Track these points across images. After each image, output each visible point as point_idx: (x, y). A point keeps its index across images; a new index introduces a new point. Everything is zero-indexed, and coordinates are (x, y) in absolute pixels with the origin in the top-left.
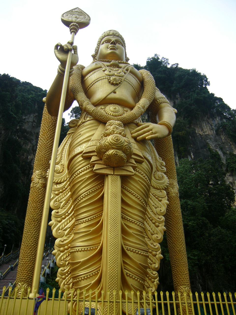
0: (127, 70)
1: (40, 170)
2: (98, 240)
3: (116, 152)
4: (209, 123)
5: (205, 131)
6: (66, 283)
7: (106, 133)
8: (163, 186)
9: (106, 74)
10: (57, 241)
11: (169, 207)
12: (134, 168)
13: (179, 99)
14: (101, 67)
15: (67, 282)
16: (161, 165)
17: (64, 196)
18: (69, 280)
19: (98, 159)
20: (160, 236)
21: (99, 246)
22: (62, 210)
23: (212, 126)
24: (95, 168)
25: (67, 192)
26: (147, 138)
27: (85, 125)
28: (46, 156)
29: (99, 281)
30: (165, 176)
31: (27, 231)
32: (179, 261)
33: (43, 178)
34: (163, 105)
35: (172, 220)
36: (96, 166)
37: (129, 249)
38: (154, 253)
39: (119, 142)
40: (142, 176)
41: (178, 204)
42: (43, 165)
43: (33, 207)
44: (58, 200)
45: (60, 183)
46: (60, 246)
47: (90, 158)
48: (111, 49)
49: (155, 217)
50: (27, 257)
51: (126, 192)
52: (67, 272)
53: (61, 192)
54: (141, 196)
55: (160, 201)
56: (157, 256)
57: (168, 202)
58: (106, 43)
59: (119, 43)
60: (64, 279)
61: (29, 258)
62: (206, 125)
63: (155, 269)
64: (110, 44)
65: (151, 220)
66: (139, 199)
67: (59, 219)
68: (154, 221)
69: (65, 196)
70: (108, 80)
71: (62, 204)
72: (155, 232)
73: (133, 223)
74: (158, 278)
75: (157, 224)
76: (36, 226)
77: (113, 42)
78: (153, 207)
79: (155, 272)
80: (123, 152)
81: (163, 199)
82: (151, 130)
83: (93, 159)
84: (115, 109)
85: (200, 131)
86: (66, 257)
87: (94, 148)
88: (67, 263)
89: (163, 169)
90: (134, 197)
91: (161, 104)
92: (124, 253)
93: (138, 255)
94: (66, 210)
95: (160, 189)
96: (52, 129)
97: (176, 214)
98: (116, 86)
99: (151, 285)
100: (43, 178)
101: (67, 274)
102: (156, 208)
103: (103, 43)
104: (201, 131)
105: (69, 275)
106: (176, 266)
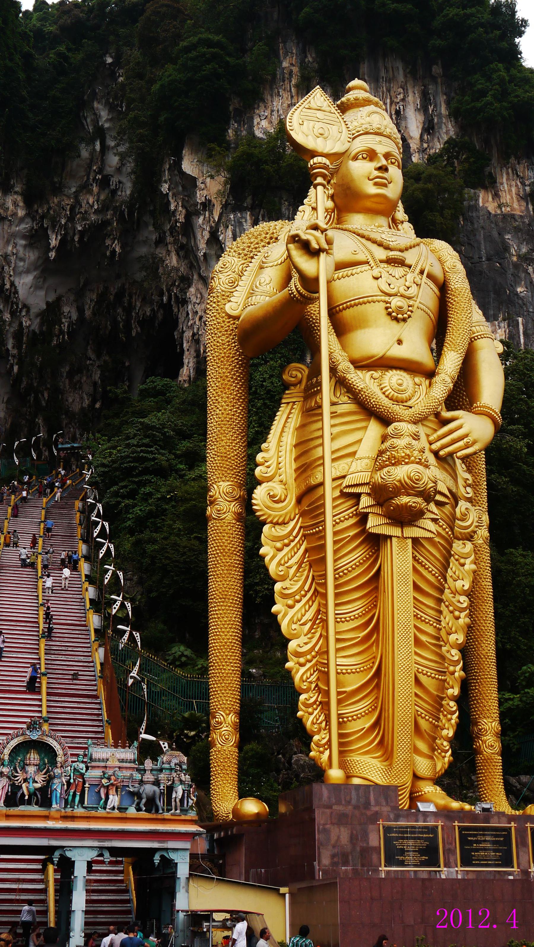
0: (422, 272)
1: (228, 481)
2: (370, 652)
3: (414, 502)
4: (517, 174)
5: (503, 200)
6: (315, 721)
7: (395, 458)
8: (468, 533)
9: (382, 291)
10: (292, 645)
12: (435, 520)
13: (439, 80)
15: (317, 720)
16: (465, 484)
17: (293, 554)
18: (320, 716)
19: (373, 503)
20: (460, 638)
21: (373, 663)
22: (292, 582)
23: (523, 184)
24: (369, 525)
25: (298, 546)
26: (459, 454)
27: (339, 412)
28: (235, 446)
31: (221, 614)
32: (484, 675)
33: (236, 500)
34: (480, 343)
35: (475, 594)
36: (370, 518)
37: (420, 670)
38: (451, 668)
39: (421, 483)
40: (443, 533)
42: (232, 470)
43: (225, 566)
44: (282, 562)
45: (284, 523)
46: (298, 655)
47: (357, 497)
48: (376, 184)
49: (453, 600)
50: (228, 665)
51: (418, 567)
52: (315, 702)
53: (287, 545)
54: (440, 572)
55: (463, 565)
56: (457, 674)
58: (364, 158)
59: (393, 161)
60: (311, 714)
61: (232, 666)
62: (508, 179)
64: (376, 169)
65: (447, 607)
66: (437, 577)
67: (290, 602)
68: (451, 608)
69: (295, 553)
70: (387, 308)
71: (292, 571)
72: (453, 629)
73: (427, 623)
74: (457, 713)
75: (457, 613)
76: (235, 604)
77: (384, 167)
78: (451, 580)
79: (452, 704)
80: (424, 499)
81: (468, 561)
82: (467, 436)
83: (365, 501)
84: (400, 385)
85: (490, 199)
86: (311, 675)
87: (365, 477)
88: (313, 686)
89: (468, 493)
90: (430, 575)
91: (476, 340)
93: (434, 680)
94: (300, 583)
95: (463, 540)
96: (239, 376)
97: (483, 584)
98: (402, 323)
99: (446, 726)
100: (236, 500)
101: (315, 706)
102: (455, 581)
103: (355, 158)
104: (493, 199)
105: (319, 708)
106: (477, 682)
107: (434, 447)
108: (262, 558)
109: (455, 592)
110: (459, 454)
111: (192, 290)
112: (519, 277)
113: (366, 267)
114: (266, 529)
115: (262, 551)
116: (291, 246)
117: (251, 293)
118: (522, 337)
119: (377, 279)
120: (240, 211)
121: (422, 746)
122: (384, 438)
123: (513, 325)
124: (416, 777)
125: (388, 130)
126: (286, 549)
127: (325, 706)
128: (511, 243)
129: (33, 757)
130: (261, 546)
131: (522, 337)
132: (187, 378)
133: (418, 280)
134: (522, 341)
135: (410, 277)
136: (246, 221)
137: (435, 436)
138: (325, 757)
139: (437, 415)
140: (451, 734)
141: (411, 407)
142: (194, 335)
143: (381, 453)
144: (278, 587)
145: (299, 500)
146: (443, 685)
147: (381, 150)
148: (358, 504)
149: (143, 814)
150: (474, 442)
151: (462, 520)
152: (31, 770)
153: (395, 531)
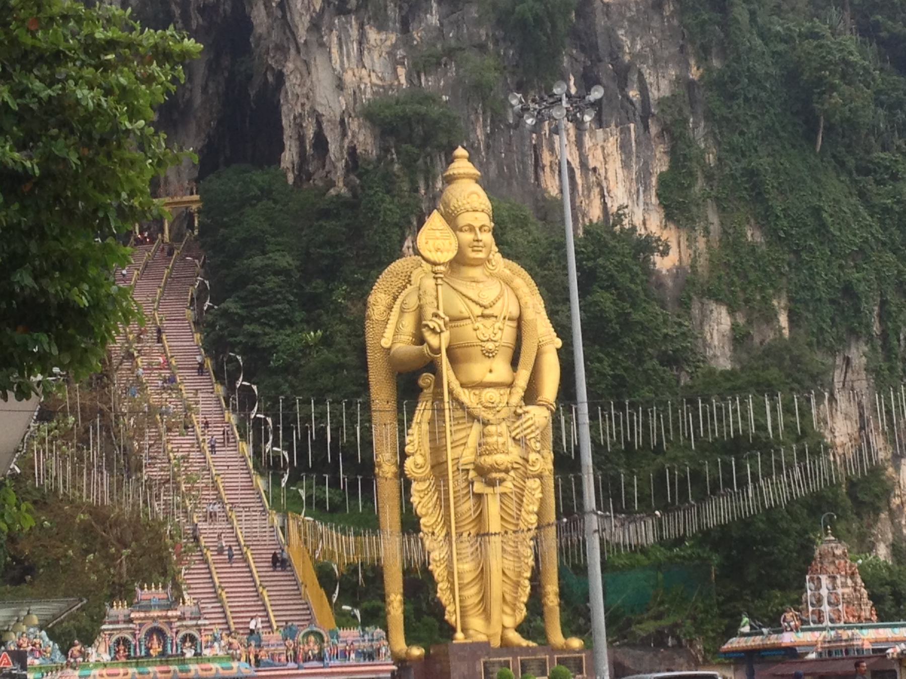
0: (504, 318)
11: (542, 501)
14: (469, 318)
26: (528, 437)
29: (482, 600)
30: (538, 456)
41: (551, 483)
45: (425, 480)
48: (473, 251)
57: (541, 495)
63: (527, 578)
71: (430, 511)
87: (471, 458)
92: (504, 573)
94: (435, 519)
107: (513, 434)
108: (412, 504)
109: (528, 513)
110: (528, 437)
111: (290, 66)
112: (631, 80)
113: (468, 321)
114: (414, 485)
115: (412, 500)
116: (424, 330)
117: (397, 332)
118: (634, 144)
119: (475, 330)
120: (344, 14)
121: (508, 610)
122: (483, 435)
123: (625, 131)
124: (504, 627)
125: (483, 207)
126: (426, 497)
127: (452, 590)
128: (624, 38)
129: (312, 638)
130: (411, 496)
131: (634, 144)
132: (290, 166)
133: (502, 327)
134: (634, 149)
135: (498, 325)
136: (351, 27)
137: (512, 428)
138: (453, 619)
139: (515, 412)
140: (525, 599)
141: (498, 411)
142: (295, 118)
143: (480, 445)
144: (422, 521)
145: (433, 467)
146: (519, 574)
147: (477, 225)
148: (468, 473)
149: (367, 662)
150: (537, 428)
151: (533, 466)
152: (311, 644)
153: (489, 490)
